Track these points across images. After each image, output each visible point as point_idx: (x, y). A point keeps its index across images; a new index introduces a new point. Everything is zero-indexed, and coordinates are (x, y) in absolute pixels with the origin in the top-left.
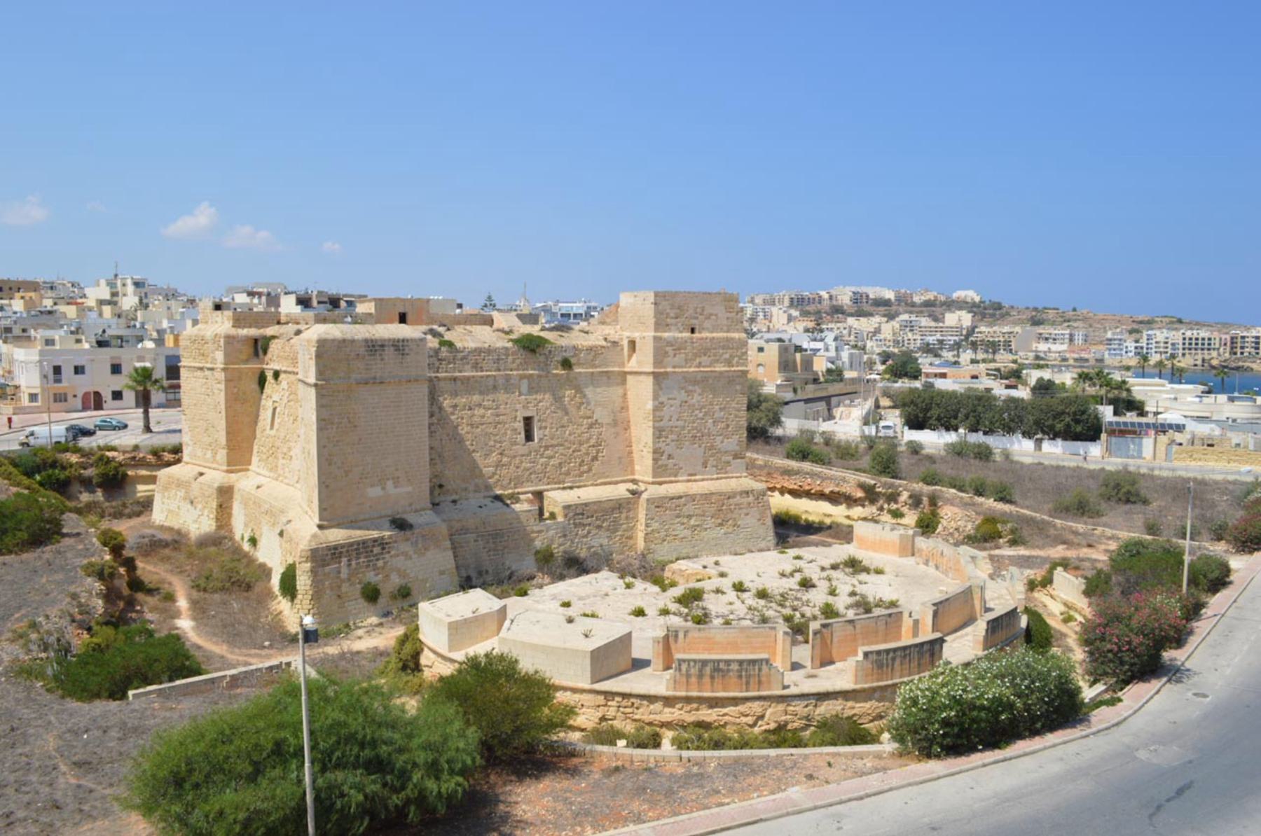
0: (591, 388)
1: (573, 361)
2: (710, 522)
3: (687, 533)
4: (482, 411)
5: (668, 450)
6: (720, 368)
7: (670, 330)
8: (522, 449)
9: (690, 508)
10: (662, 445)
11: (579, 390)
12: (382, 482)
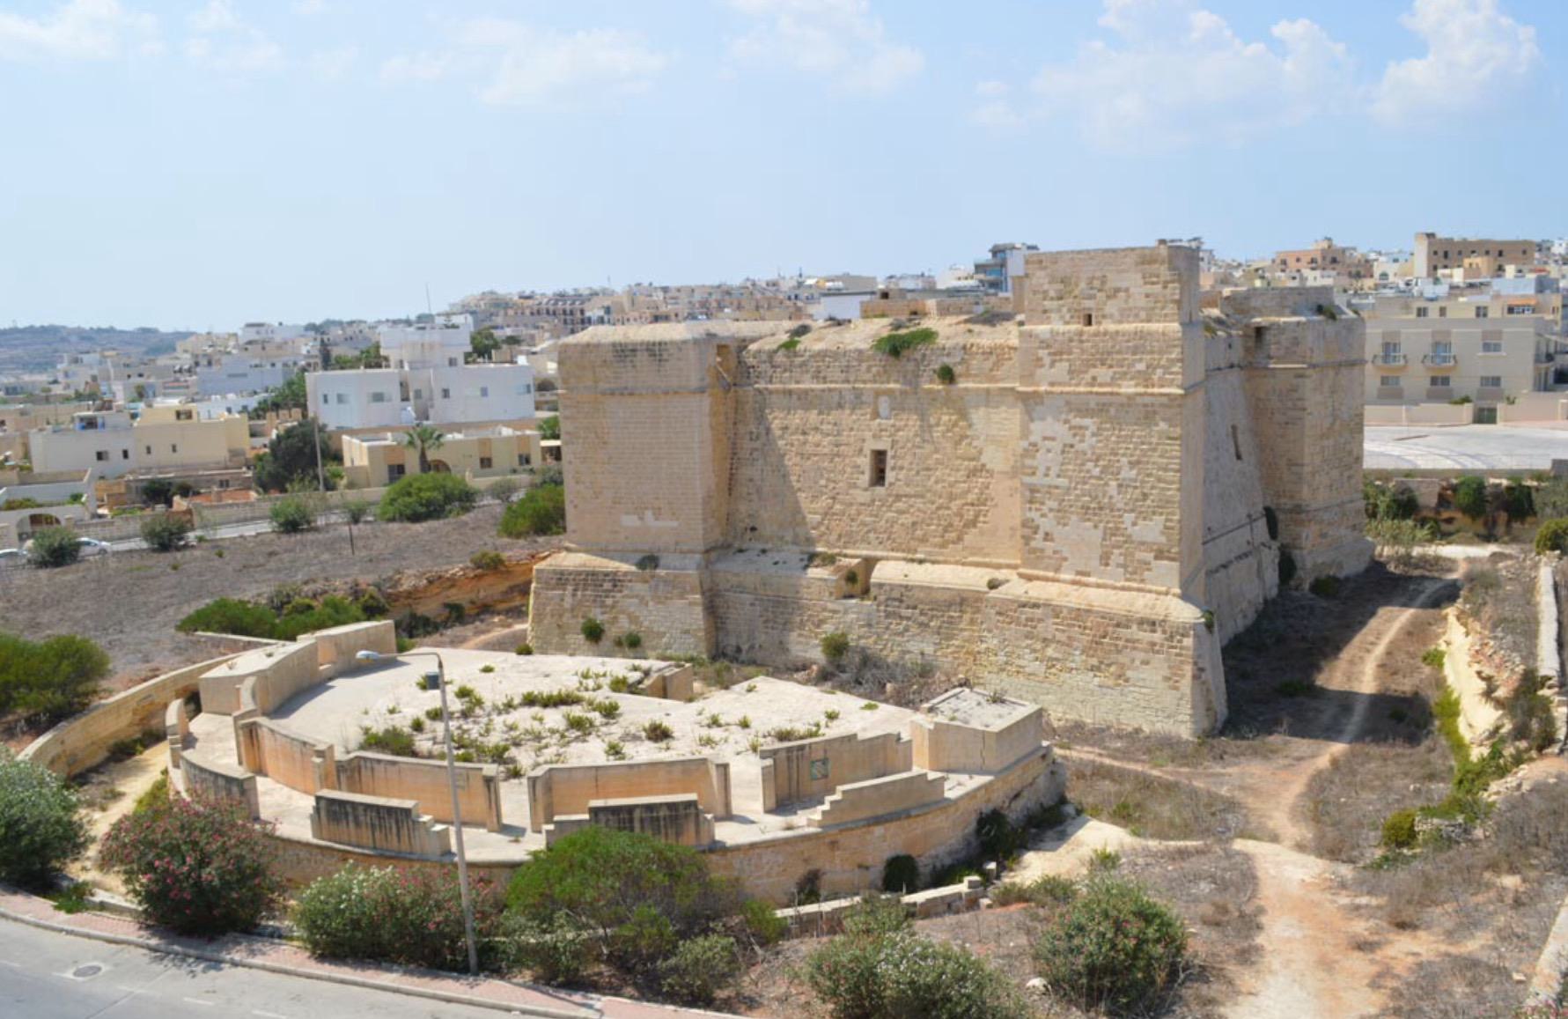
0: (982, 411)
1: (958, 370)
2: (1078, 658)
3: (1036, 667)
4: (818, 437)
5: (1046, 524)
6: (1128, 388)
7: (1048, 321)
8: (863, 496)
9: (1048, 627)
10: (1034, 515)
11: (963, 414)
12: (639, 511)
